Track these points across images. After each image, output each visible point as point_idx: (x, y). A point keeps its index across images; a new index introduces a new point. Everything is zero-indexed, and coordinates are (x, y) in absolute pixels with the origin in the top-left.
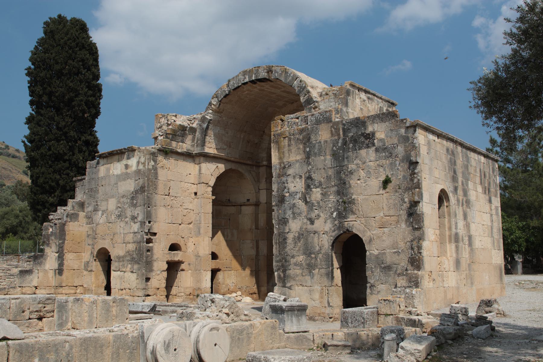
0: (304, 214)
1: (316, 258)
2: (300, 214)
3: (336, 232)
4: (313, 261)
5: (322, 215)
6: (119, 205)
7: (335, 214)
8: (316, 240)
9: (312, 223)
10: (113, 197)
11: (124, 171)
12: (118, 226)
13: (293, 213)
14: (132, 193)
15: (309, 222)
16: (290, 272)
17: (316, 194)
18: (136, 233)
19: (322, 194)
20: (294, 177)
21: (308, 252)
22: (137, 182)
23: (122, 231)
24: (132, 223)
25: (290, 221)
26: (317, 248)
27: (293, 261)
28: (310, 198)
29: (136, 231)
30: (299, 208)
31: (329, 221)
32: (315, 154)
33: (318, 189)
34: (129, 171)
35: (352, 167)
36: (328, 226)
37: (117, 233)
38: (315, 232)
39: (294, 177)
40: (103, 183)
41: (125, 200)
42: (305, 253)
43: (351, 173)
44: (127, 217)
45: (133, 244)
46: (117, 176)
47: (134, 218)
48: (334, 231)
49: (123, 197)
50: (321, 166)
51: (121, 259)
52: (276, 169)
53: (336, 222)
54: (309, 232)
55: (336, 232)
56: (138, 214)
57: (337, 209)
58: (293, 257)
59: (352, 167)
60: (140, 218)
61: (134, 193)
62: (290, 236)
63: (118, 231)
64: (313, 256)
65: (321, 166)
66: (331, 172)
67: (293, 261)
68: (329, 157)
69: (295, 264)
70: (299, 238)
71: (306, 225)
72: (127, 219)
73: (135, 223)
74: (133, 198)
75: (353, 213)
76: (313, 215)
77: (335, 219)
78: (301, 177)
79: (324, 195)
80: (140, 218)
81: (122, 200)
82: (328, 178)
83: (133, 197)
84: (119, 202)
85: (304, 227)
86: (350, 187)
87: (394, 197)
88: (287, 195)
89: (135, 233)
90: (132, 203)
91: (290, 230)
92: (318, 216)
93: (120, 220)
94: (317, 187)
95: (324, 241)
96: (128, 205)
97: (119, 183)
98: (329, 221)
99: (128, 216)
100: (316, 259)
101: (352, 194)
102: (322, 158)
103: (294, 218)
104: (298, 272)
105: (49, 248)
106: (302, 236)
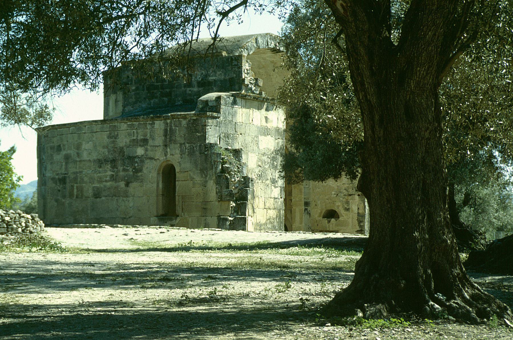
6: (260, 163)
11: (264, 123)
18: (277, 198)
22: (277, 141)
29: (276, 196)
34: (269, 125)
40: (243, 132)
41: (265, 158)
44: (268, 179)
45: (274, 211)
73: (275, 187)
83: (273, 157)
84: (260, 160)
89: (275, 198)
90: (273, 164)
93: (261, 181)
96: (268, 165)
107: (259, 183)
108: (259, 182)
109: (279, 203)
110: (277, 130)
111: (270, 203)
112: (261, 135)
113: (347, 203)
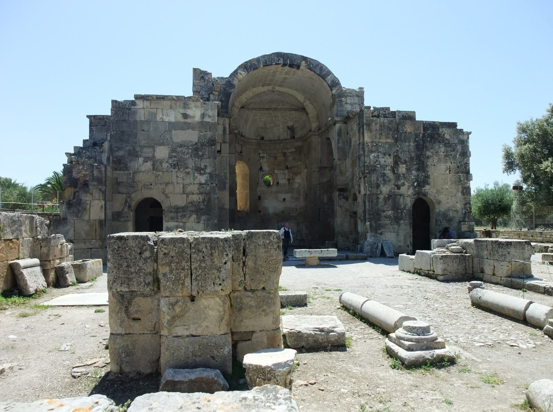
0: (393, 182)
1: (402, 213)
2: (389, 181)
3: (416, 196)
4: (399, 215)
5: (406, 183)
6: (174, 154)
7: (416, 184)
8: (401, 200)
9: (399, 187)
10: (163, 144)
12: (174, 177)
13: (384, 180)
14: (196, 144)
15: (396, 188)
16: (381, 222)
17: (402, 169)
18: (204, 184)
19: (406, 169)
20: (385, 154)
21: (396, 207)
23: (180, 181)
24: (196, 174)
25: (382, 186)
26: (402, 206)
27: (383, 214)
28: (397, 170)
29: (203, 181)
30: (388, 177)
31: (411, 188)
32: (402, 141)
33: (404, 166)
35: (428, 153)
36: (411, 191)
37: (172, 183)
38: (401, 195)
39: (385, 154)
41: (184, 149)
42: (393, 209)
43: (428, 157)
44: (187, 168)
45: (200, 196)
46: (170, 123)
47: (199, 170)
48: (414, 195)
49: (181, 146)
50: (406, 149)
51: (180, 210)
52: (368, 146)
53: (417, 189)
54: (396, 195)
55: (416, 196)
56: (206, 166)
57: (417, 180)
58: (384, 211)
59: (428, 153)
60: (208, 171)
61: (199, 144)
62: (381, 197)
63: (174, 181)
64: (399, 211)
65: (406, 149)
66: (413, 155)
67: (383, 214)
68: (412, 144)
69: (386, 217)
70: (388, 198)
71: (394, 189)
72: (188, 170)
73: (201, 174)
74: (196, 149)
75: (429, 184)
76: (399, 183)
77: (415, 187)
78: (390, 155)
79: (408, 170)
80: (208, 171)
81: (179, 149)
82: (412, 158)
84: (173, 150)
85: (393, 191)
86: (427, 166)
87: (455, 177)
88: (379, 166)
89: (201, 184)
91: (381, 192)
92: (403, 184)
93: (176, 170)
94: (403, 164)
95: (408, 202)
97: (173, 132)
98: (411, 188)
99: (190, 166)
100: (402, 214)
101: (428, 172)
102: (407, 144)
103: (384, 184)
104: (388, 222)
105: (88, 195)
106: (392, 197)
107: (174, 173)
108: (174, 170)
109: (208, 188)
110: (203, 125)
111: (194, 188)
112: (175, 130)
113: (359, 186)
